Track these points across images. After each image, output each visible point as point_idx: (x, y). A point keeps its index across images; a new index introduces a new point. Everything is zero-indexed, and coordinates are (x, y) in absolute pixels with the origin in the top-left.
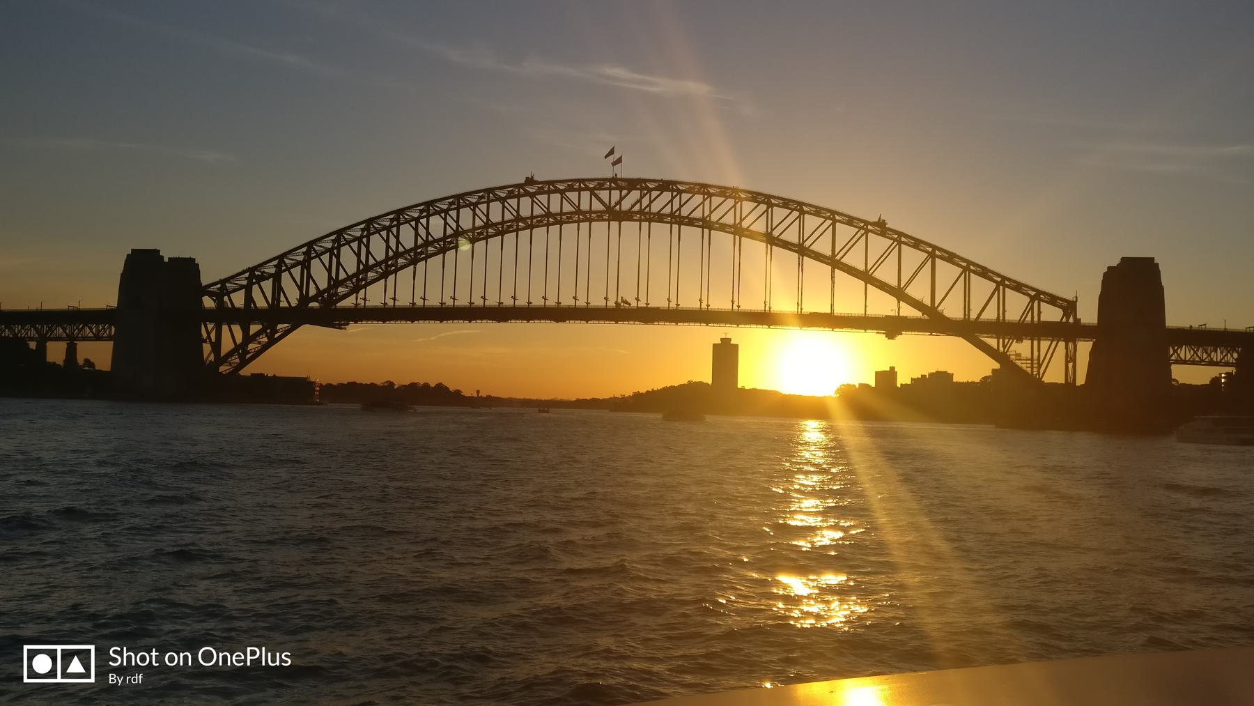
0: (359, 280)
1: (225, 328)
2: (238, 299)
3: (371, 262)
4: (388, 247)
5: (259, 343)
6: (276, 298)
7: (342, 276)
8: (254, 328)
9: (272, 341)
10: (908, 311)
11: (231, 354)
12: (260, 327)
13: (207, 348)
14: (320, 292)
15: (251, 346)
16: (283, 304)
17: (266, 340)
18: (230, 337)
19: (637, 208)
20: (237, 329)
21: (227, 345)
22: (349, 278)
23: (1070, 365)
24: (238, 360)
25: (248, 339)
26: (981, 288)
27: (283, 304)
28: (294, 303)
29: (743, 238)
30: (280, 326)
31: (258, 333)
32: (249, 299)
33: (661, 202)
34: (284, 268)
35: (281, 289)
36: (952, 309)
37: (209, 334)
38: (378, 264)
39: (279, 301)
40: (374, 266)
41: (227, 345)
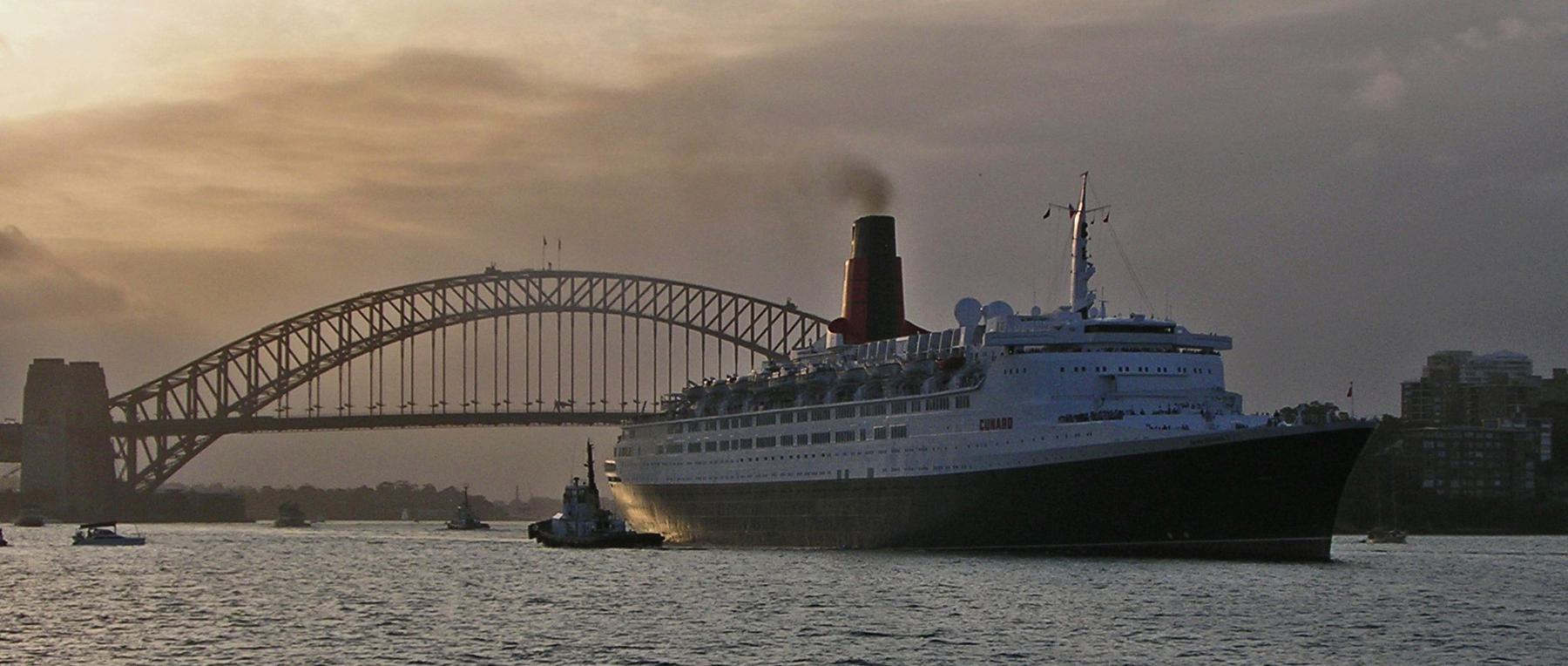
0: (281, 385)
1: (139, 442)
9: (191, 455)
11: (147, 470)
13: (120, 464)
15: (168, 461)
16: (202, 415)
18: (147, 451)
20: (152, 441)
21: (142, 463)
24: (154, 477)
27: (202, 415)
28: (213, 415)
30: (198, 438)
35: (197, 397)
39: (196, 411)
41: (142, 463)
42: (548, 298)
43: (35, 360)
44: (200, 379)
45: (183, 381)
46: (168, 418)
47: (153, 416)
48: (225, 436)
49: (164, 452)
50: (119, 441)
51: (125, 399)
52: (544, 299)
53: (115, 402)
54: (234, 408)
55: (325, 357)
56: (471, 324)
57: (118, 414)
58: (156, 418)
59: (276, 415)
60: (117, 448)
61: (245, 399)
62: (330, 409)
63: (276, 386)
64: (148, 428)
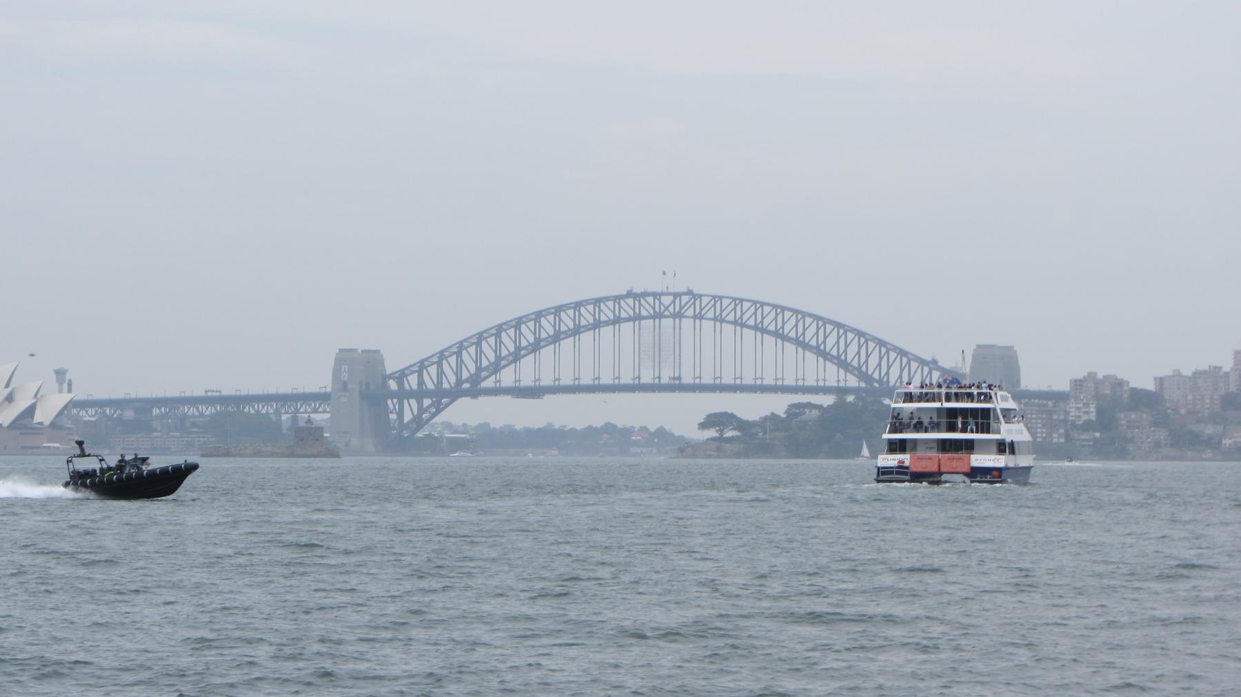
1: (405, 401)
5: (430, 413)
6: (440, 383)
9: (439, 411)
11: (411, 422)
13: (393, 416)
14: (471, 376)
15: (424, 416)
16: (446, 385)
18: (410, 409)
20: (413, 402)
21: (408, 417)
27: (446, 385)
29: (744, 329)
31: (429, 407)
39: (441, 383)
41: (408, 417)
42: (667, 308)
43: (340, 350)
44: (444, 362)
45: (434, 363)
46: (424, 387)
47: (415, 387)
48: (461, 399)
49: (421, 410)
50: (393, 402)
51: (397, 375)
52: (662, 308)
53: (390, 377)
54: (466, 381)
55: (525, 348)
56: (617, 326)
57: (393, 385)
59: (493, 385)
60: (391, 406)
62: (527, 382)
64: (411, 394)
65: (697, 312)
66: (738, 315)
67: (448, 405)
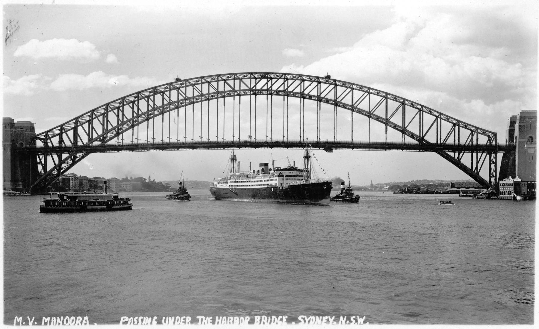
0: (119, 129)
2: (55, 141)
3: (125, 119)
4: (133, 112)
5: (68, 163)
7: (110, 127)
8: (65, 156)
9: (74, 163)
10: (409, 140)
12: (68, 155)
13: (40, 167)
14: (99, 137)
15: (63, 166)
16: (80, 143)
17: (71, 162)
18: (52, 162)
19: (265, 88)
20: (55, 156)
21: (50, 165)
22: (114, 128)
23: (493, 166)
25: (61, 161)
26: (447, 126)
27: (80, 143)
30: (78, 155)
31: (67, 159)
32: (61, 141)
33: (277, 85)
34: (79, 124)
36: (431, 138)
37: (40, 160)
38: (129, 121)
40: (126, 122)
41: (50, 165)
46: (63, 145)
57: (39, 144)
58: (58, 145)
60: (38, 160)
61: (101, 136)
63: (116, 129)
65: (302, 91)
66: (286, 87)
67: (83, 157)
